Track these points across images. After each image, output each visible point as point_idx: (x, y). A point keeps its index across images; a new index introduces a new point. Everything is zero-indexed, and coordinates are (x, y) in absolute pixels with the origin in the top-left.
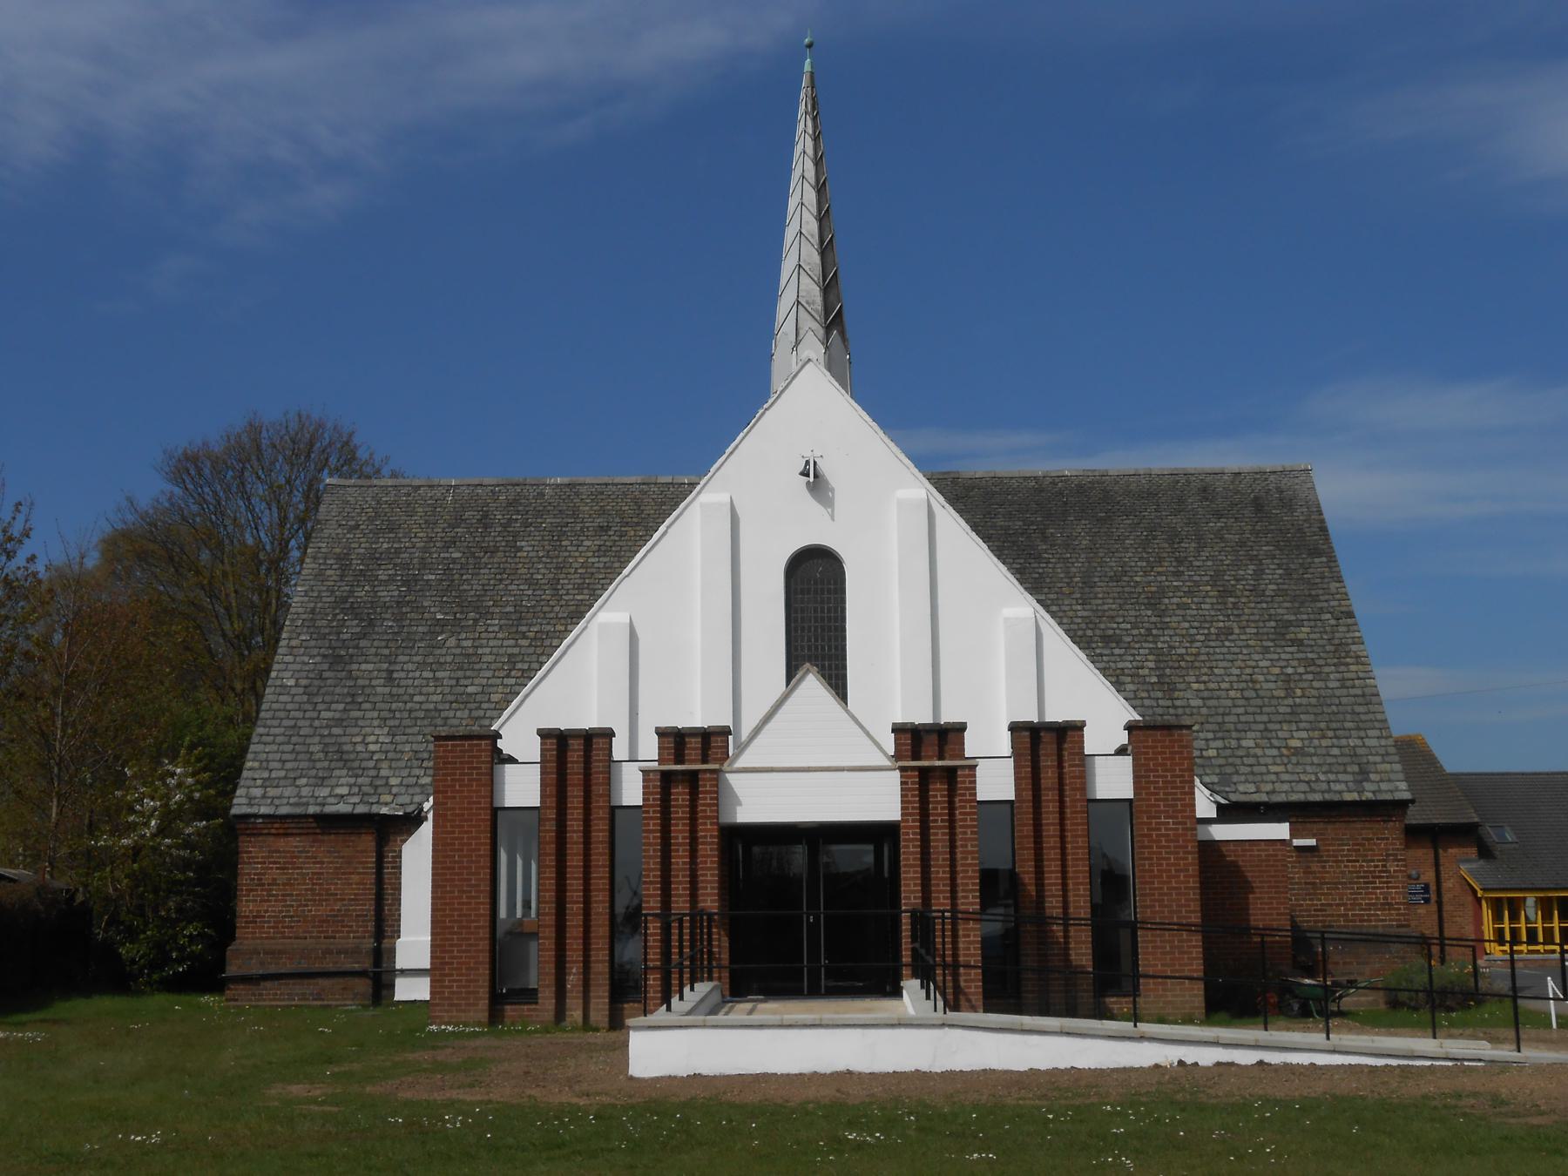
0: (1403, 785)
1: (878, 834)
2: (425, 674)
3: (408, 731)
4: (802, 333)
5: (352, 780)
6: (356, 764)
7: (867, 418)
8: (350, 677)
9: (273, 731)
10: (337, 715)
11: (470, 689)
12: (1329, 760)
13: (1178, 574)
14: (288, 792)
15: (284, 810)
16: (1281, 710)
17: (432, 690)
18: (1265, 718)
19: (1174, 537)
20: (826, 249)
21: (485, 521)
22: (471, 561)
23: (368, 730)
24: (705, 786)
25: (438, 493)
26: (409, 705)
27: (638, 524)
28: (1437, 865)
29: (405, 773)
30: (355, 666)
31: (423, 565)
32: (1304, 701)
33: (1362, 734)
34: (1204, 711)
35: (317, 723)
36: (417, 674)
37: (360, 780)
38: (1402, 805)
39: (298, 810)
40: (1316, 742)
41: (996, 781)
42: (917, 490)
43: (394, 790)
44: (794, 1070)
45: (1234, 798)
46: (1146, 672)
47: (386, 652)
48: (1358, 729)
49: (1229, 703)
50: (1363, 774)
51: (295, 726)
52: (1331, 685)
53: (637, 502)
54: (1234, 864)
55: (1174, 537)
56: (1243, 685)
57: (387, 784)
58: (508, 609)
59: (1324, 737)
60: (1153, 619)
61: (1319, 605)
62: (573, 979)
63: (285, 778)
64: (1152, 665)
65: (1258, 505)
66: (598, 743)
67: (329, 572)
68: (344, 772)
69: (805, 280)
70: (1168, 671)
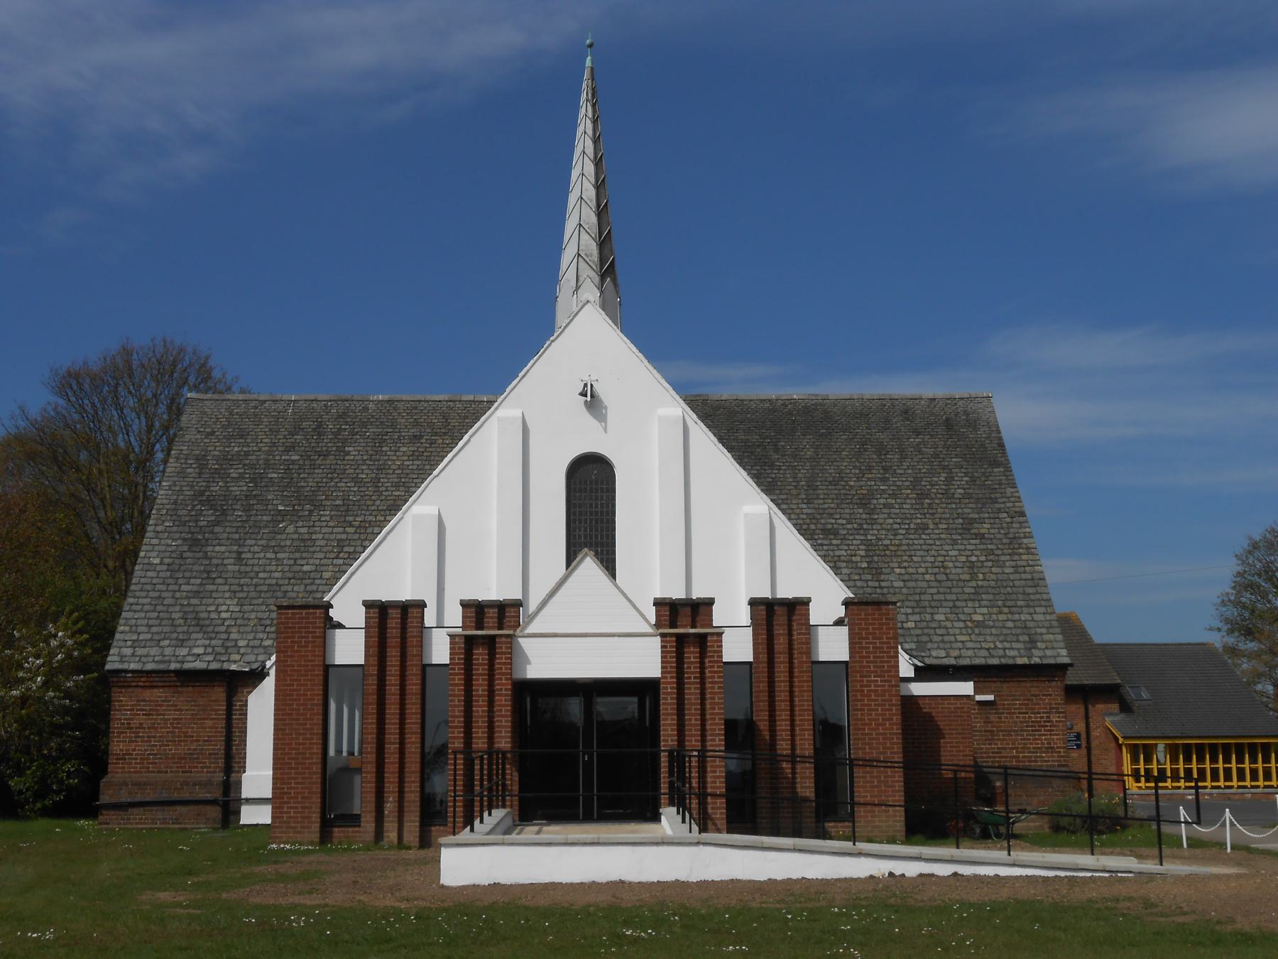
0: (1064, 652)
1: (642, 689)
2: (268, 555)
3: (255, 602)
4: (581, 279)
5: (207, 642)
6: (210, 629)
7: (634, 349)
8: (206, 557)
9: (141, 601)
10: (195, 588)
11: (306, 568)
12: (1005, 631)
13: (884, 480)
14: (154, 651)
15: (149, 667)
16: (967, 590)
17: (274, 568)
18: (954, 597)
19: (881, 450)
20: (602, 212)
22: (307, 462)
23: (221, 601)
24: (501, 647)
25: (280, 406)
26: (255, 581)
27: (445, 434)
28: (1087, 717)
29: (251, 636)
30: (210, 548)
31: (268, 465)
32: (985, 583)
33: (1032, 610)
34: (905, 591)
35: (178, 595)
36: (262, 555)
37: (213, 642)
38: (1063, 668)
39: (162, 667)
40: (994, 617)
41: (738, 646)
42: (674, 409)
43: (242, 651)
44: (576, 880)
45: (928, 661)
46: (858, 559)
47: (237, 536)
48: (1028, 606)
49: (925, 584)
50: (1032, 643)
51: (159, 597)
52: (1007, 571)
53: (445, 417)
54: (930, 715)
55: (881, 450)
56: (936, 570)
57: (236, 645)
58: (338, 502)
59: (1001, 613)
60: (864, 516)
61: (997, 506)
62: (390, 806)
63: (151, 640)
64: (863, 553)
65: (949, 424)
66: (413, 612)
67: (189, 470)
68: (200, 635)
69: (584, 236)
70: (876, 559)
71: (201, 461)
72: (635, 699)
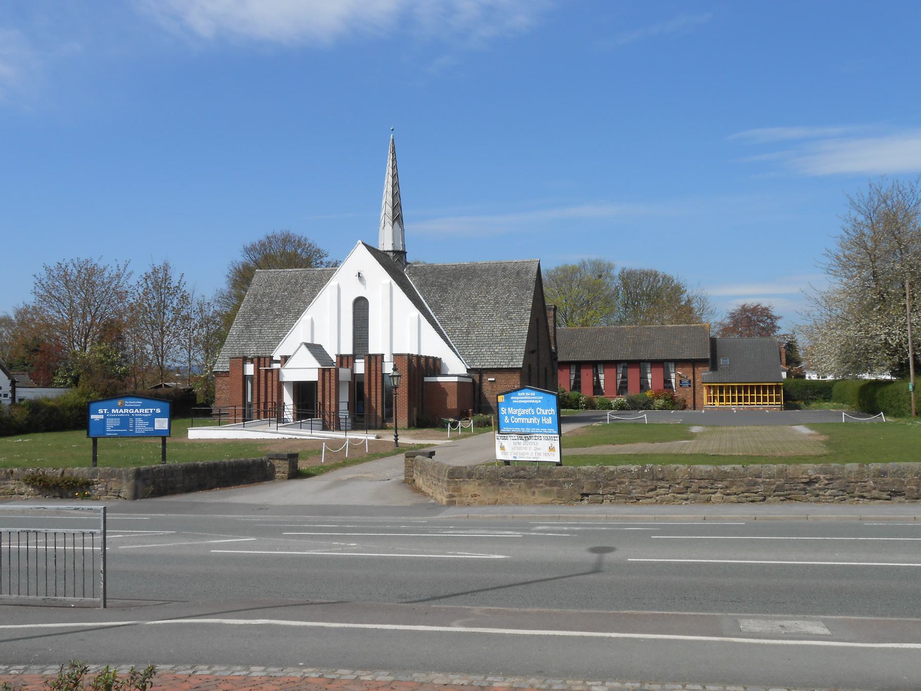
21: (296, 283)
28: (694, 373)
65: (518, 273)
71: (255, 295)
72: (520, 365)
